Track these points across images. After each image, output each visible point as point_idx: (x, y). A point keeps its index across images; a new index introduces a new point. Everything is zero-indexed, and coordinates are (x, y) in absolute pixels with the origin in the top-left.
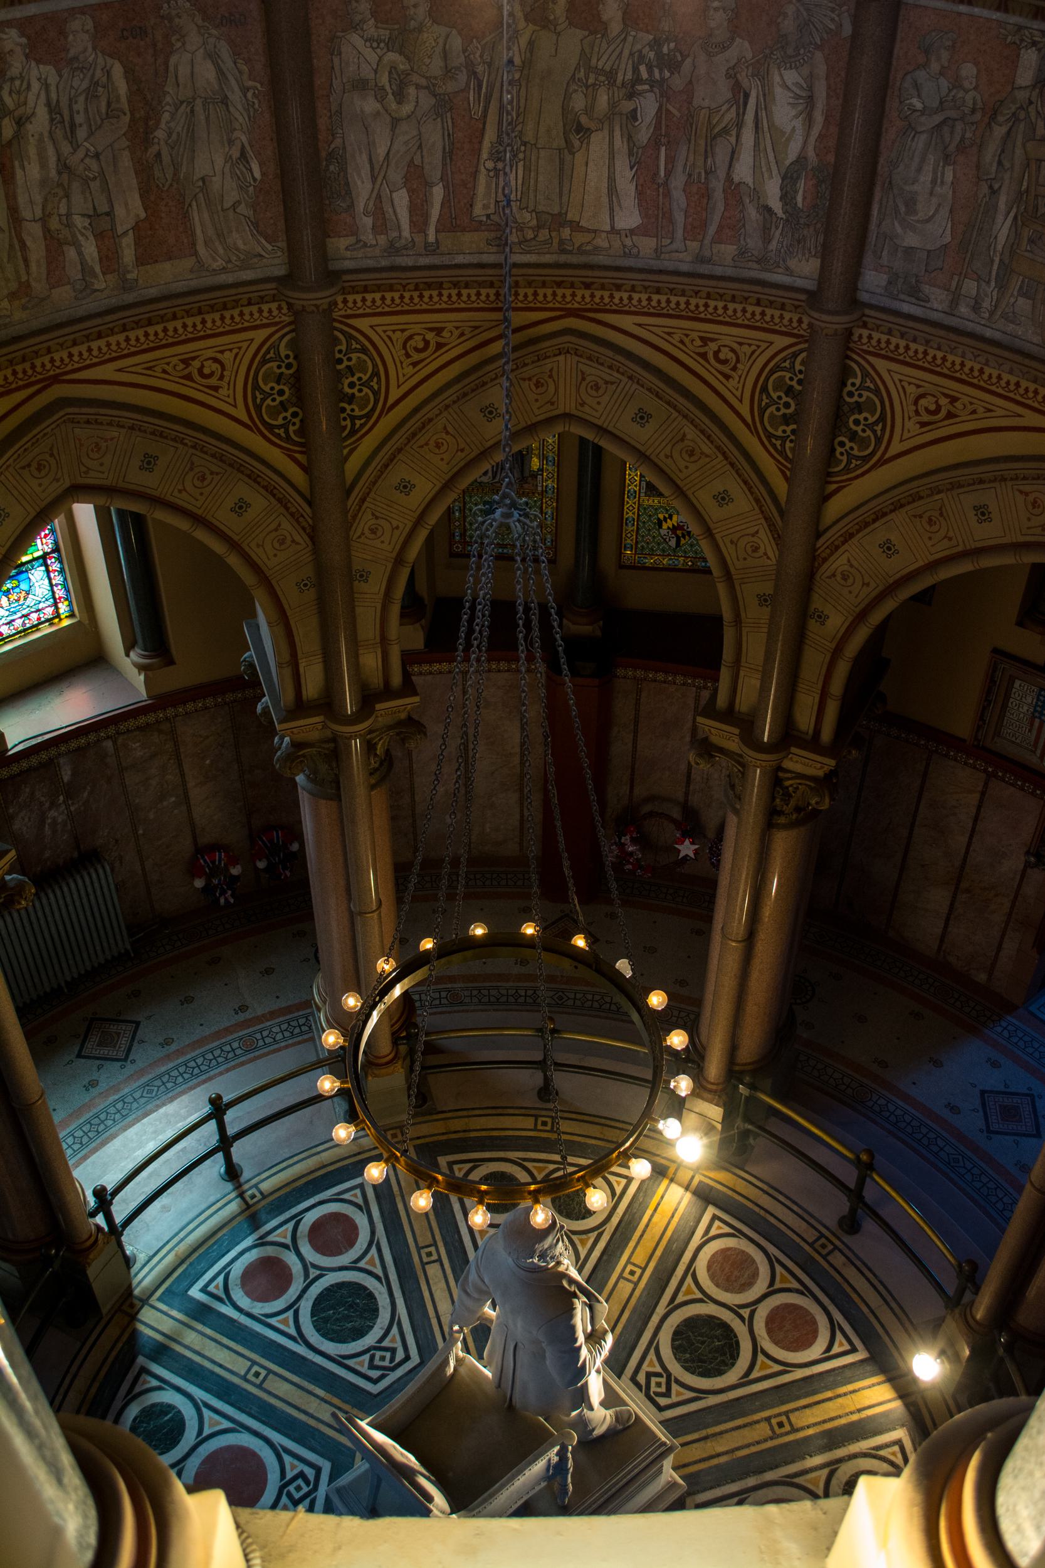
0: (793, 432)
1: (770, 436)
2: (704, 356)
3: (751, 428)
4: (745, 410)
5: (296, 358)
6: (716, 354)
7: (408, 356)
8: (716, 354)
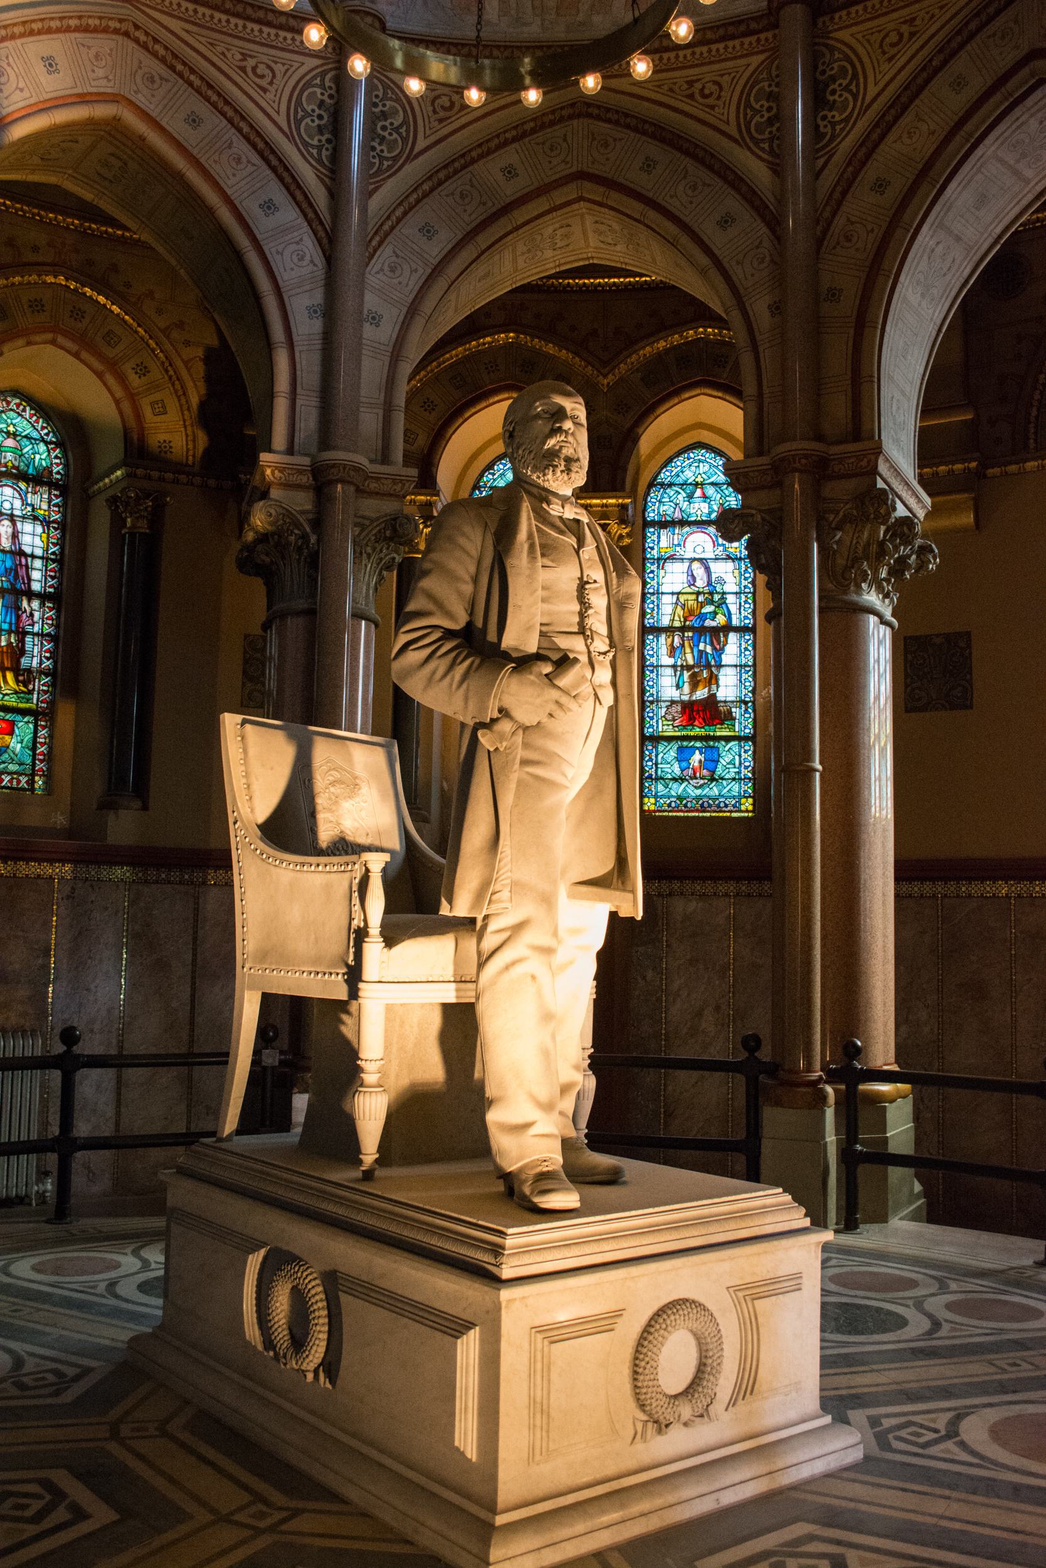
1: (306, 144)
2: (243, 69)
3: (290, 138)
4: (282, 120)
6: (254, 69)
8: (254, 69)
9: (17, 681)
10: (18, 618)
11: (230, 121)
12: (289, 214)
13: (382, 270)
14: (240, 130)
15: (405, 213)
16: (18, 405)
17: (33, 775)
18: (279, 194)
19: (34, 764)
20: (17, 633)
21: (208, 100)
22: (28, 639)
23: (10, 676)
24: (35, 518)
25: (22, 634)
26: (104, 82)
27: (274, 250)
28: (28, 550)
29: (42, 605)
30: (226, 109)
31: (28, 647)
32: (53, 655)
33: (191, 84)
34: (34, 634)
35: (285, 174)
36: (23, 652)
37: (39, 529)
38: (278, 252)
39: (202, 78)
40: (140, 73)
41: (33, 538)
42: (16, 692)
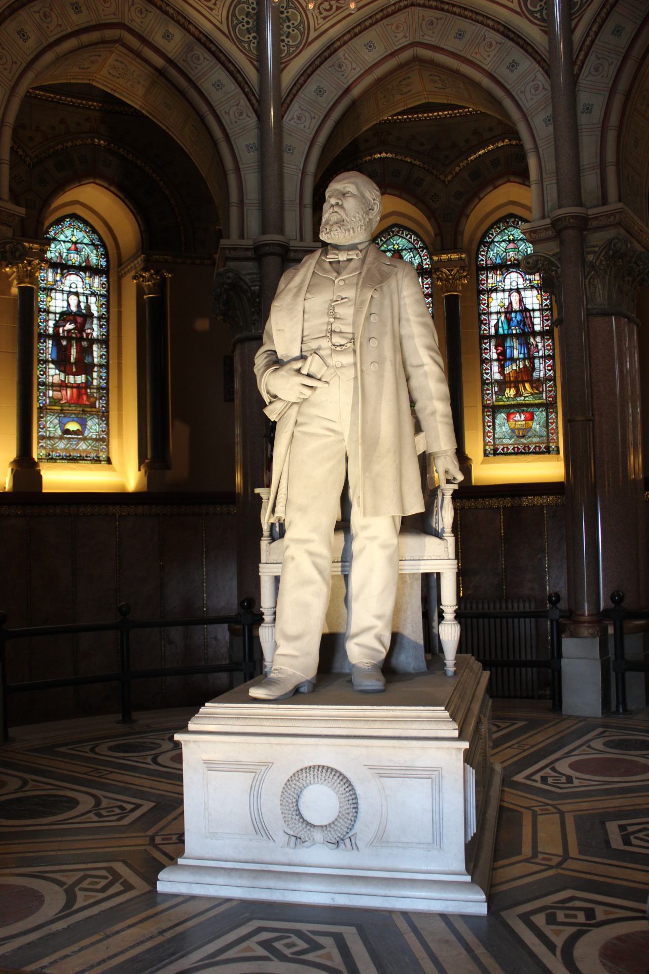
0: (545, 4)
5: (257, 4)
7: (321, 13)
9: (532, 388)
10: (529, 350)
11: (482, 23)
12: (527, 64)
13: (590, 73)
14: (488, 26)
15: (600, 27)
16: (513, 222)
17: (548, 442)
18: (517, 54)
19: (548, 436)
20: (529, 358)
21: (466, 17)
22: (536, 361)
23: (527, 385)
24: (532, 287)
25: (532, 359)
26: (404, 40)
27: (519, 92)
28: (530, 307)
29: (543, 338)
30: (478, 17)
31: (537, 365)
32: (553, 368)
33: (454, 13)
34: (540, 357)
35: (519, 40)
36: (533, 369)
37: (535, 292)
38: (522, 92)
39: (460, 7)
40: (424, 22)
41: (532, 300)
42: (532, 394)
